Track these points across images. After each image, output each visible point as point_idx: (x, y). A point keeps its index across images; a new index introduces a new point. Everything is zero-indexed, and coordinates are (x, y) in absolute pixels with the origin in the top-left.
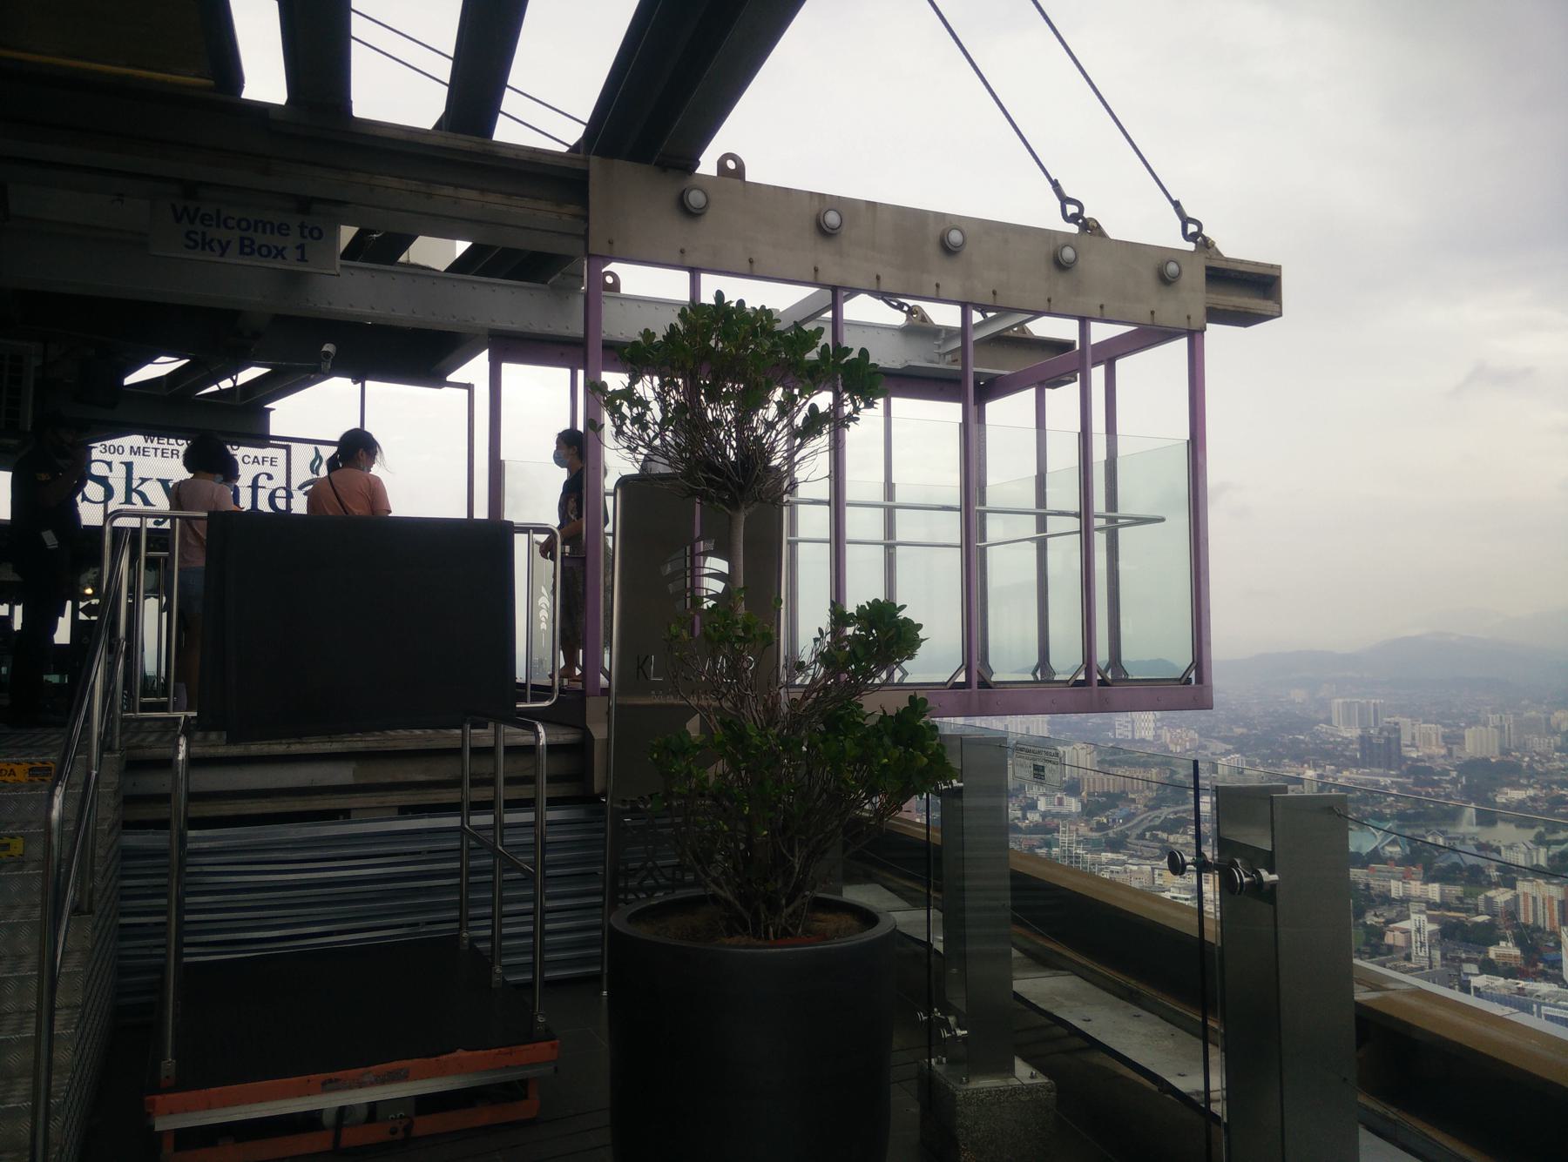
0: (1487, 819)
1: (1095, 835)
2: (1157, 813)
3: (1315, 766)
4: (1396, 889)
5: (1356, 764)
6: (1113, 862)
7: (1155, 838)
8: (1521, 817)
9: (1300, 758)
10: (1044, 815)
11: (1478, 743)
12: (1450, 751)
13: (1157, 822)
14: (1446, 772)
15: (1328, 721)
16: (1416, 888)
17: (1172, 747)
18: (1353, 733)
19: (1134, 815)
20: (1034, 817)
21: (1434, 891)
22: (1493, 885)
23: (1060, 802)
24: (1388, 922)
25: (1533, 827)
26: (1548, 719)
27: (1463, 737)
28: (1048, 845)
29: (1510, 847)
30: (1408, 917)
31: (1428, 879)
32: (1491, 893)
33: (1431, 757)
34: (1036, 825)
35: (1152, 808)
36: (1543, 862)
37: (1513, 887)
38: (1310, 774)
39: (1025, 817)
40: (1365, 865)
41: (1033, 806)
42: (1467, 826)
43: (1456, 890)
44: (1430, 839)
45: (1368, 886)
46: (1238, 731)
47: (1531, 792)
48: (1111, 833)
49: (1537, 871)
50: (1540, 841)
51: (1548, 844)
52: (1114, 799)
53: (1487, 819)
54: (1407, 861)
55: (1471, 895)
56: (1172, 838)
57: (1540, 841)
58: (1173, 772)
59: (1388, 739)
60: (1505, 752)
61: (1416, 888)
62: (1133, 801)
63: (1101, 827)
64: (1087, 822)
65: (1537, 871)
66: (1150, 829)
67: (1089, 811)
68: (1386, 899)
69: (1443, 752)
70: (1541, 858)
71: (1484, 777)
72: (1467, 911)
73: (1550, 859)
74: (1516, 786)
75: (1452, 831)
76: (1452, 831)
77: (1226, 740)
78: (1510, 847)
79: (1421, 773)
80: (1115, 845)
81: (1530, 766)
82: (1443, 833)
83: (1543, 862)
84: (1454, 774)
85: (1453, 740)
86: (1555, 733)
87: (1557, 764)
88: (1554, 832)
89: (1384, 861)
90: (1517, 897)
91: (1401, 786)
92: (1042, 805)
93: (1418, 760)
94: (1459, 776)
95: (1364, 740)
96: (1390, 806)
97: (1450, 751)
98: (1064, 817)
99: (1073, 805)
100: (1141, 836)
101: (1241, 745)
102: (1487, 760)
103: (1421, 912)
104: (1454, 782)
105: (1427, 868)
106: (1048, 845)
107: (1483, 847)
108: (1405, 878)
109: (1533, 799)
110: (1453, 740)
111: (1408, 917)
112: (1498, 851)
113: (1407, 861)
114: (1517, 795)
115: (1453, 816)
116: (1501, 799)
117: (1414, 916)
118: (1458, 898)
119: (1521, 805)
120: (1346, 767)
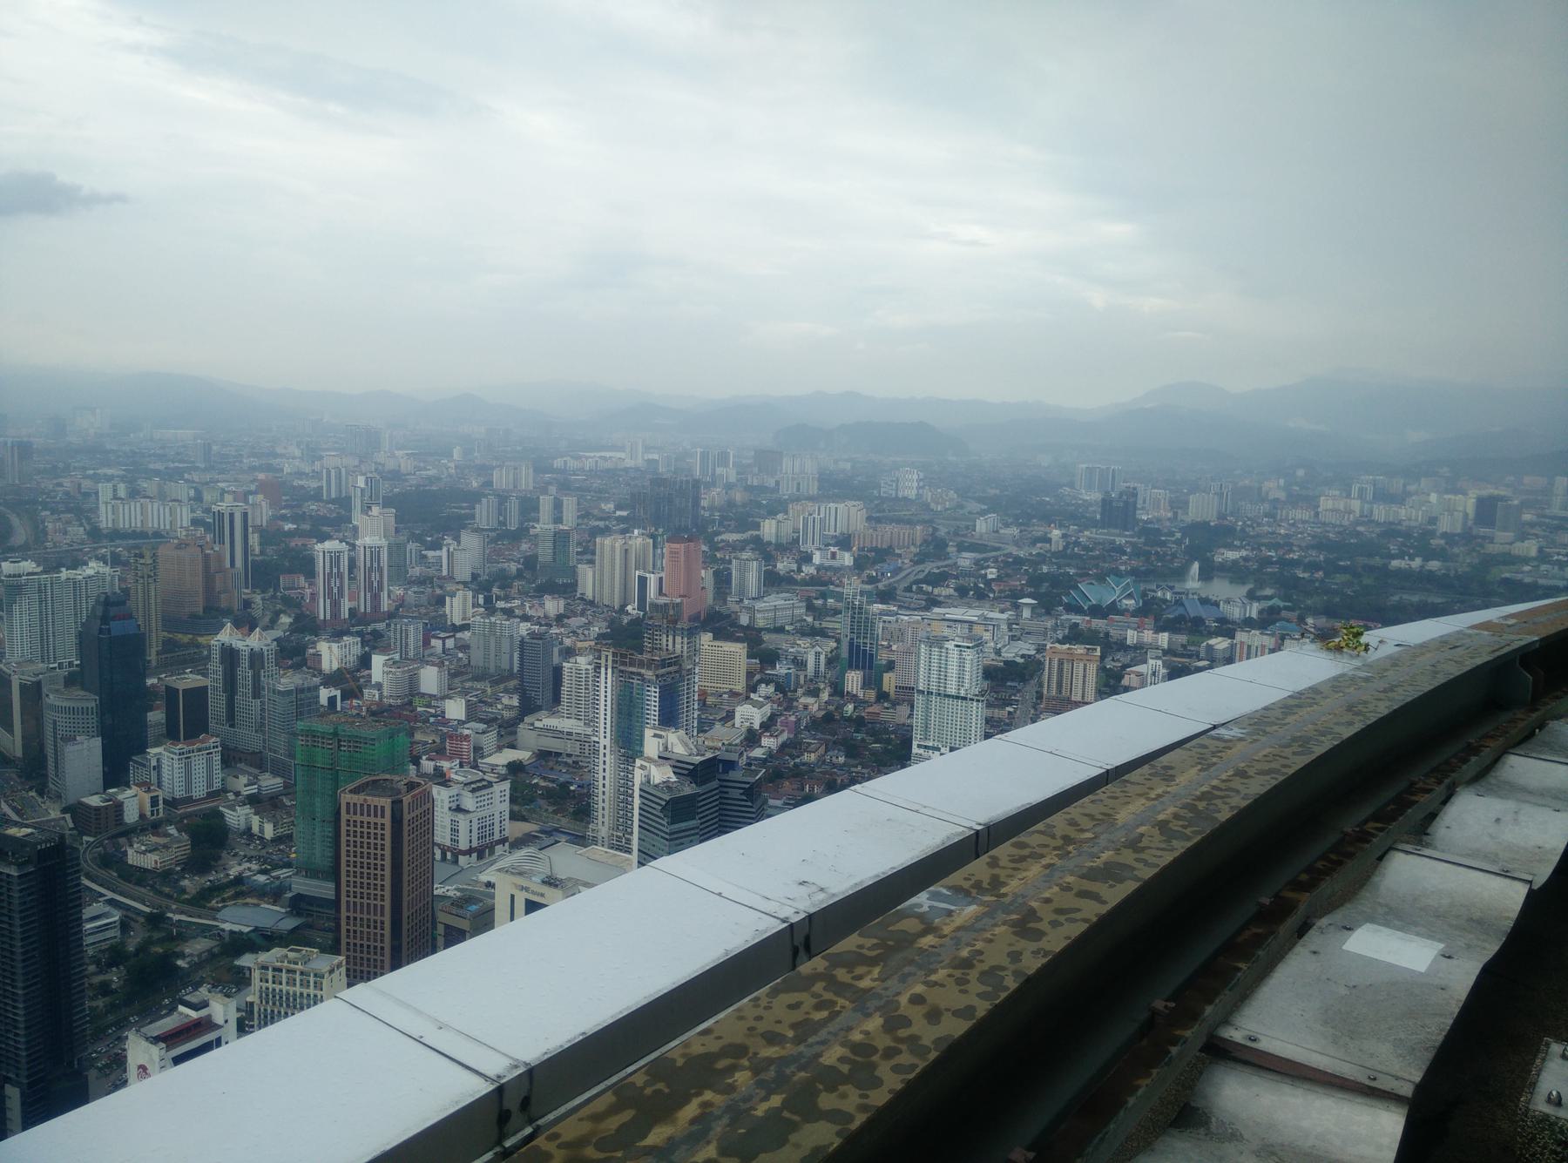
0: (1206, 575)
1: (868, 587)
2: (921, 567)
3: (1061, 526)
4: (1132, 637)
5: (1094, 524)
6: (882, 613)
7: (920, 590)
8: (1236, 573)
9: (1048, 518)
10: (818, 568)
11: (1201, 509)
12: (1176, 514)
13: (921, 576)
14: (1171, 534)
15: (1071, 485)
16: (1148, 636)
17: (933, 506)
18: (1095, 496)
19: (900, 569)
20: (808, 570)
21: (1164, 639)
22: (1211, 634)
23: (834, 555)
24: (1125, 667)
25: (1244, 583)
26: (1260, 489)
27: (1187, 503)
28: (824, 596)
29: (1228, 601)
30: (1145, 662)
31: (1159, 629)
32: (1212, 642)
33: (1159, 520)
34: (812, 577)
35: (916, 563)
36: (1254, 615)
37: (1233, 637)
38: (1056, 533)
39: (800, 570)
40: (1104, 617)
41: (807, 558)
42: (1193, 583)
43: (1182, 639)
44: (1159, 594)
45: (1107, 634)
46: (992, 492)
47: (1244, 553)
48: (881, 586)
49: (1248, 623)
50: (1252, 596)
51: (1259, 599)
52: (882, 554)
53: (1206, 575)
54: (1141, 612)
55: (1193, 644)
56: (936, 591)
57: (1252, 596)
58: (935, 530)
59: (1126, 503)
60: (1222, 517)
61: (1148, 636)
62: (900, 556)
63: (872, 580)
64: (859, 576)
65: (1248, 623)
66: (917, 582)
67: (860, 564)
68: (1122, 646)
69: (1170, 515)
70: (1254, 610)
71: (1203, 541)
72: (1190, 656)
73: (1260, 612)
74: (1231, 547)
75: (1178, 587)
76: (1178, 587)
77: (980, 500)
78: (1228, 601)
79: (1151, 534)
80: (886, 596)
81: (1243, 530)
82: (1172, 588)
83: (1254, 615)
84: (1178, 535)
85: (1178, 504)
86: (1263, 500)
87: (1266, 528)
88: (1262, 588)
89: (1121, 613)
90: (1233, 646)
91: (1133, 545)
92: (817, 559)
93: (1149, 522)
94: (1184, 537)
95: (1106, 503)
96: (1125, 563)
97: (1176, 514)
98: (836, 570)
99: (847, 559)
100: (908, 589)
101: (993, 505)
102: (1207, 523)
103: (1157, 658)
104: (1179, 542)
105: (1156, 620)
106: (824, 596)
107: (1205, 601)
108: (1139, 628)
109: (1246, 559)
110: (1178, 504)
111: (1145, 662)
112: (1217, 604)
113: (1141, 612)
114: (1232, 555)
115: (1181, 574)
116: (1218, 559)
117: (1151, 662)
118: (1184, 646)
119: (1235, 562)
120: (1086, 528)
